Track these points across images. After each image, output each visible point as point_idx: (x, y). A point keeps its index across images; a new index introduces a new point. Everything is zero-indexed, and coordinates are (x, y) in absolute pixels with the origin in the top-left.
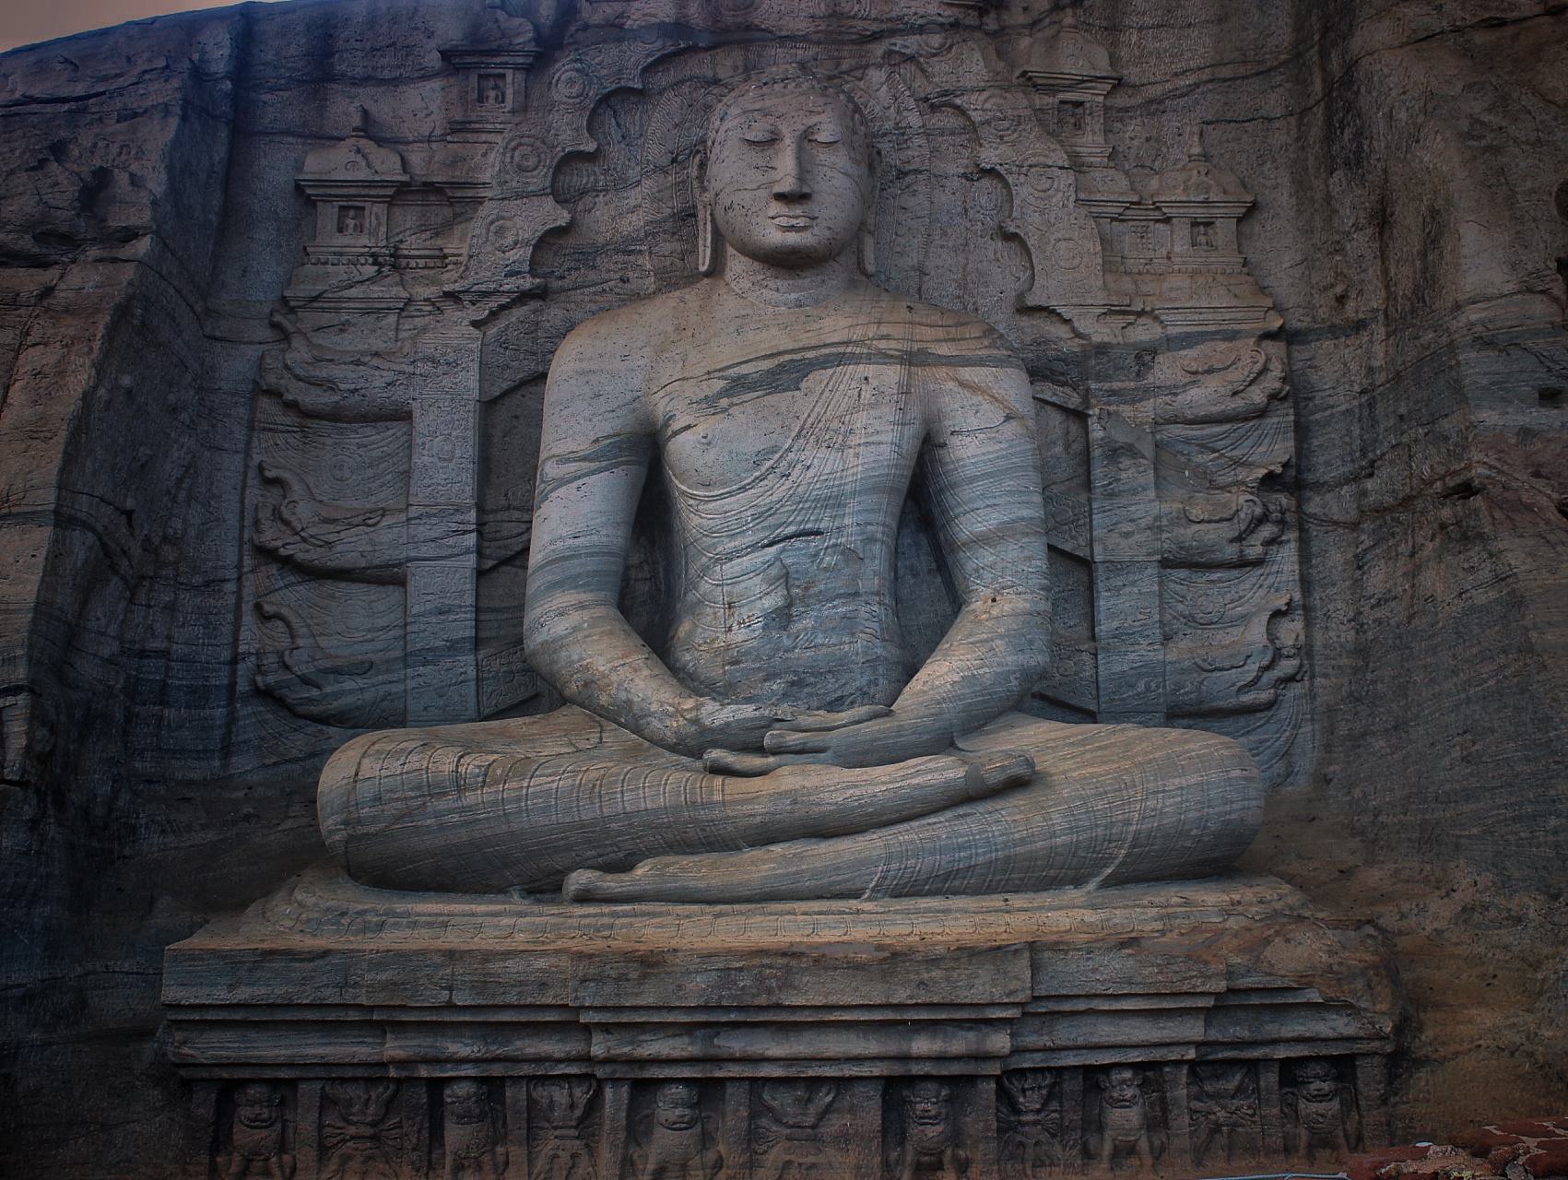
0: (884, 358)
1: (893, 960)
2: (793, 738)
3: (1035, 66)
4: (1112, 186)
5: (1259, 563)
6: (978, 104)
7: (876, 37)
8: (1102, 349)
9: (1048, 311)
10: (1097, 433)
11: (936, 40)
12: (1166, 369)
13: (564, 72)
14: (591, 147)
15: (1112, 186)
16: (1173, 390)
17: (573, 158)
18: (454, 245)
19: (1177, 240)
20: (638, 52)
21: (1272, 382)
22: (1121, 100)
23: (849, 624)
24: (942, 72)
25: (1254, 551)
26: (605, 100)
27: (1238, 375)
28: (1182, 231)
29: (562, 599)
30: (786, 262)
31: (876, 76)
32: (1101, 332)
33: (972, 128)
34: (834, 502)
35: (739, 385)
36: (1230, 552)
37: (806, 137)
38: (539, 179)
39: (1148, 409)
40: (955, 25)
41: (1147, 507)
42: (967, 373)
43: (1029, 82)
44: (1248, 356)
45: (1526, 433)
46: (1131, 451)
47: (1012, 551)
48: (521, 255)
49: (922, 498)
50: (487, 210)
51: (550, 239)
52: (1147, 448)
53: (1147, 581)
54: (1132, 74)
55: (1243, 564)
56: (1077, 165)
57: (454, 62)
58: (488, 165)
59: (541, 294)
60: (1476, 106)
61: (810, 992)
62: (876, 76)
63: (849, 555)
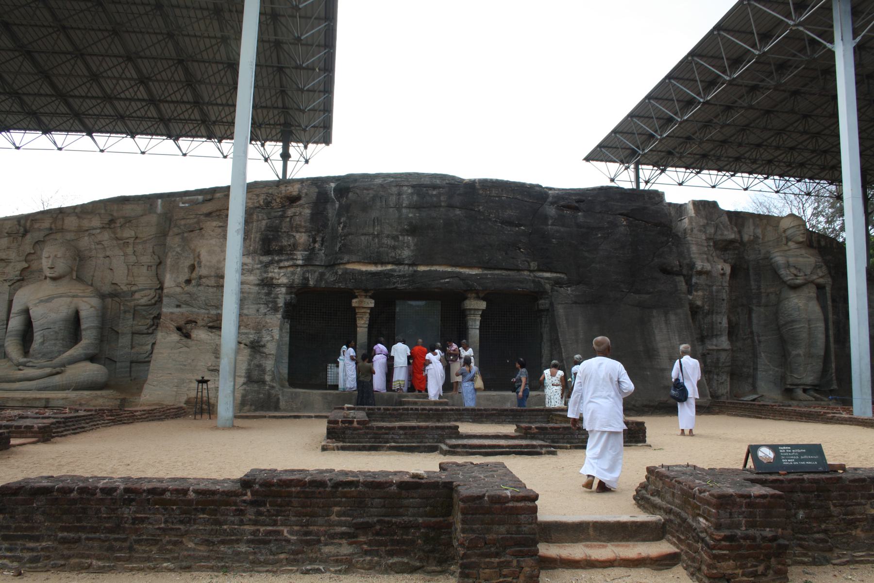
0: (69, 296)
1: (24, 400)
2: (31, 364)
3: (119, 235)
4: (132, 259)
5: (152, 333)
6: (105, 243)
7: (87, 230)
8: (124, 292)
9: (116, 284)
10: (122, 308)
11: (98, 231)
12: (137, 296)
13: (28, 236)
14: (32, 251)
15: (132, 259)
16: (138, 300)
17: (30, 254)
18: (6, 270)
19: (144, 270)
20: (42, 234)
21: (156, 299)
22: (138, 241)
23: (55, 345)
24: (99, 237)
25: (150, 331)
26: (37, 242)
27: (150, 297)
28: (145, 268)
29: (10, 338)
30: (54, 279)
31: (86, 238)
32: (125, 288)
33: (104, 248)
34: (54, 323)
35: (41, 301)
36: (146, 331)
37: (56, 256)
38: (23, 258)
39: (133, 303)
40: (103, 228)
41: (130, 322)
42: (84, 299)
43: (117, 239)
44: (152, 293)
45: (172, 313)
46: (129, 312)
47: (88, 332)
48: (18, 273)
49: (75, 320)
50: (12, 264)
51: (24, 269)
52: (132, 311)
53: (129, 337)
54: (140, 235)
55: (148, 334)
56: (125, 255)
57: (9, 234)
58: (12, 255)
59: (23, 280)
60: (178, 249)
61: (10, 404)
62: (86, 238)
63: (56, 332)
